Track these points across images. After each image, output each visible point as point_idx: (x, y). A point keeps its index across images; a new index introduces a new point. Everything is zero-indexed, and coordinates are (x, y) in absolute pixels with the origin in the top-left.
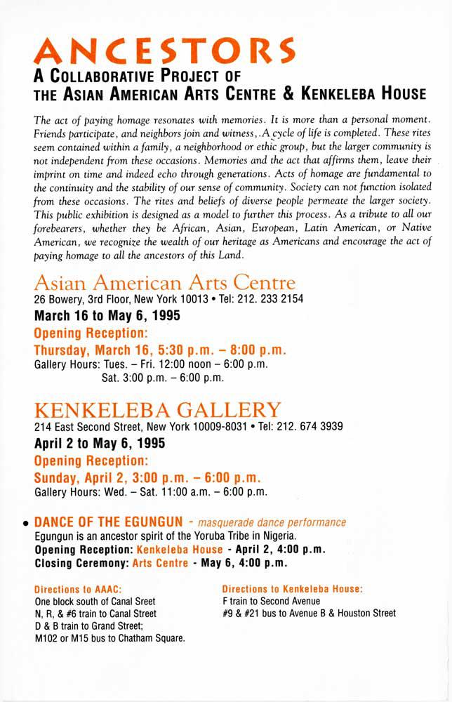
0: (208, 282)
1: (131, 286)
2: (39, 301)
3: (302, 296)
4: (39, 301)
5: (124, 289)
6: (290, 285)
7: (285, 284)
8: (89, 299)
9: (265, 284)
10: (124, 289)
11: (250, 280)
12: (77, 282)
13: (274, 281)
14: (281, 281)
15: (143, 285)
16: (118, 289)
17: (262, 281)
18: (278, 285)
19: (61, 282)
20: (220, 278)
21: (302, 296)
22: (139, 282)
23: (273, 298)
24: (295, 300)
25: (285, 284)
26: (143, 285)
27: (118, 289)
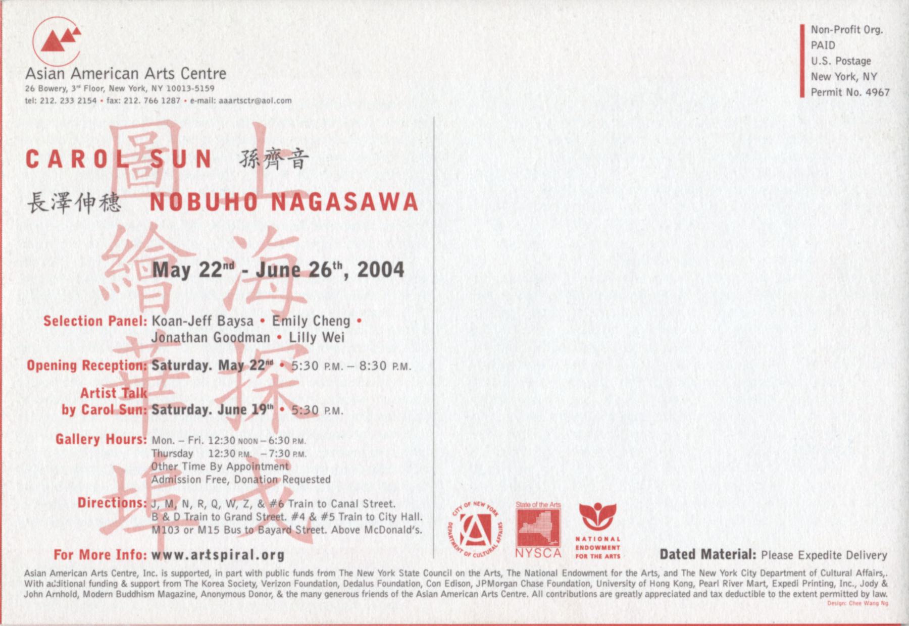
19: (46, 72)
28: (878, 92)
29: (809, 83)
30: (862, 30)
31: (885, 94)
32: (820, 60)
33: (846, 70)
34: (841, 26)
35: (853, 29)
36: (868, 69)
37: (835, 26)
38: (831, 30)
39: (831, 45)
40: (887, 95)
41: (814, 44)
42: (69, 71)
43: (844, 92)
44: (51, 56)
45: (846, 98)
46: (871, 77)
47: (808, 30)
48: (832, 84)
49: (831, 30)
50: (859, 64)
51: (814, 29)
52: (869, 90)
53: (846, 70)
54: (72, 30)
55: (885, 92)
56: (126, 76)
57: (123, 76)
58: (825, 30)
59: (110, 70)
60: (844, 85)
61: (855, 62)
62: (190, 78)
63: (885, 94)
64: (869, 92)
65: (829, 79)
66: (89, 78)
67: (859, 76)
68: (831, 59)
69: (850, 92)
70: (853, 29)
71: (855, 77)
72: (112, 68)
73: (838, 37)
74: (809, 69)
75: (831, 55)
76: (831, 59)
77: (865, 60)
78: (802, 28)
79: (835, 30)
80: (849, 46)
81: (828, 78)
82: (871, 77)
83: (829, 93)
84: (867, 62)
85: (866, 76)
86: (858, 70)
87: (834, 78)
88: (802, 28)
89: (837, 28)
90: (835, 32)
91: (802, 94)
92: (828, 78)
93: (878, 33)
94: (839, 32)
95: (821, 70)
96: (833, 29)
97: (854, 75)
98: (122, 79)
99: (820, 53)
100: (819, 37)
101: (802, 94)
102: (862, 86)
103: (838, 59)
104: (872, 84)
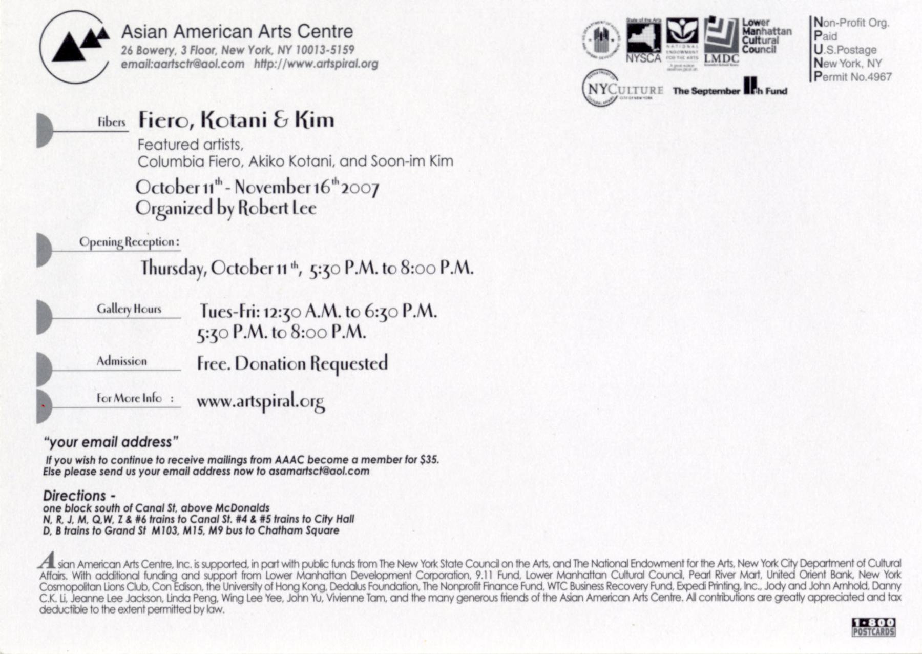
28: (880, 77)
30: (867, 23)
31: (887, 78)
33: (851, 58)
34: (848, 19)
35: (860, 22)
36: (872, 57)
37: (841, 19)
38: (838, 23)
40: (888, 80)
43: (849, 77)
45: (850, 84)
46: (876, 64)
49: (838, 23)
50: (863, 53)
52: (871, 74)
53: (851, 58)
54: (96, 33)
55: (887, 76)
56: (237, 35)
57: (234, 34)
60: (849, 71)
61: (858, 50)
62: (311, 36)
63: (887, 78)
64: (871, 78)
65: (835, 66)
66: (193, 37)
70: (860, 22)
71: (860, 64)
72: (220, 25)
77: (869, 48)
79: (841, 23)
82: (876, 64)
83: (836, 77)
86: (862, 59)
87: (839, 65)
90: (841, 26)
94: (845, 25)
96: (839, 22)
97: (859, 62)
98: (232, 38)
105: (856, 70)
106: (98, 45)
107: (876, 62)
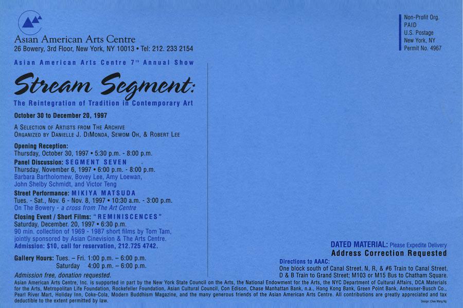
0: (95, 39)
1: (59, 41)
2: (17, 49)
3: (192, 47)
4: (17, 49)
5: (56, 42)
6: (133, 41)
7: (130, 40)
8: (48, 49)
9: (121, 40)
10: (56, 42)
11: (114, 38)
12: (34, 39)
13: (125, 38)
14: (129, 39)
15: (65, 40)
16: (53, 42)
17: (120, 39)
18: (127, 40)
20: (100, 37)
21: (192, 47)
22: (63, 39)
23: (174, 48)
24: (188, 49)
25: (130, 40)
26: (65, 40)
27: (53, 42)
29: (403, 44)
30: (429, 18)
32: (408, 33)
35: (424, 17)
36: (432, 36)
39: (414, 25)
41: (405, 24)
42: (40, 37)
44: (28, 30)
47: (403, 17)
48: (414, 44)
51: (406, 17)
58: (411, 17)
59: (65, 38)
60: (420, 45)
67: (427, 40)
68: (414, 32)
69: (423, 48)
70: (424, 17)
73: (418, 21)
74: (403, 36)
75: (414, 29)
76: (414, 32)
78: (400, 16)
80: (422, 25)
81: (412, 41)
84: (431, 33)
85: (430, 40)
86: (427, 37)
87: (415, 40)
88: (400, 16)
89: (417, 16)
91: (400, 49)
92: (412, 41)
93: (437, 20)
95: (408, 37)
99: (409, 29)
100: (407, 21)
101: (400, 49)
102: (428, 45)
103: (417, 32)
104: (433, 44)
105: (423, 44)
106: (38, 22)
107: (433, 40)
